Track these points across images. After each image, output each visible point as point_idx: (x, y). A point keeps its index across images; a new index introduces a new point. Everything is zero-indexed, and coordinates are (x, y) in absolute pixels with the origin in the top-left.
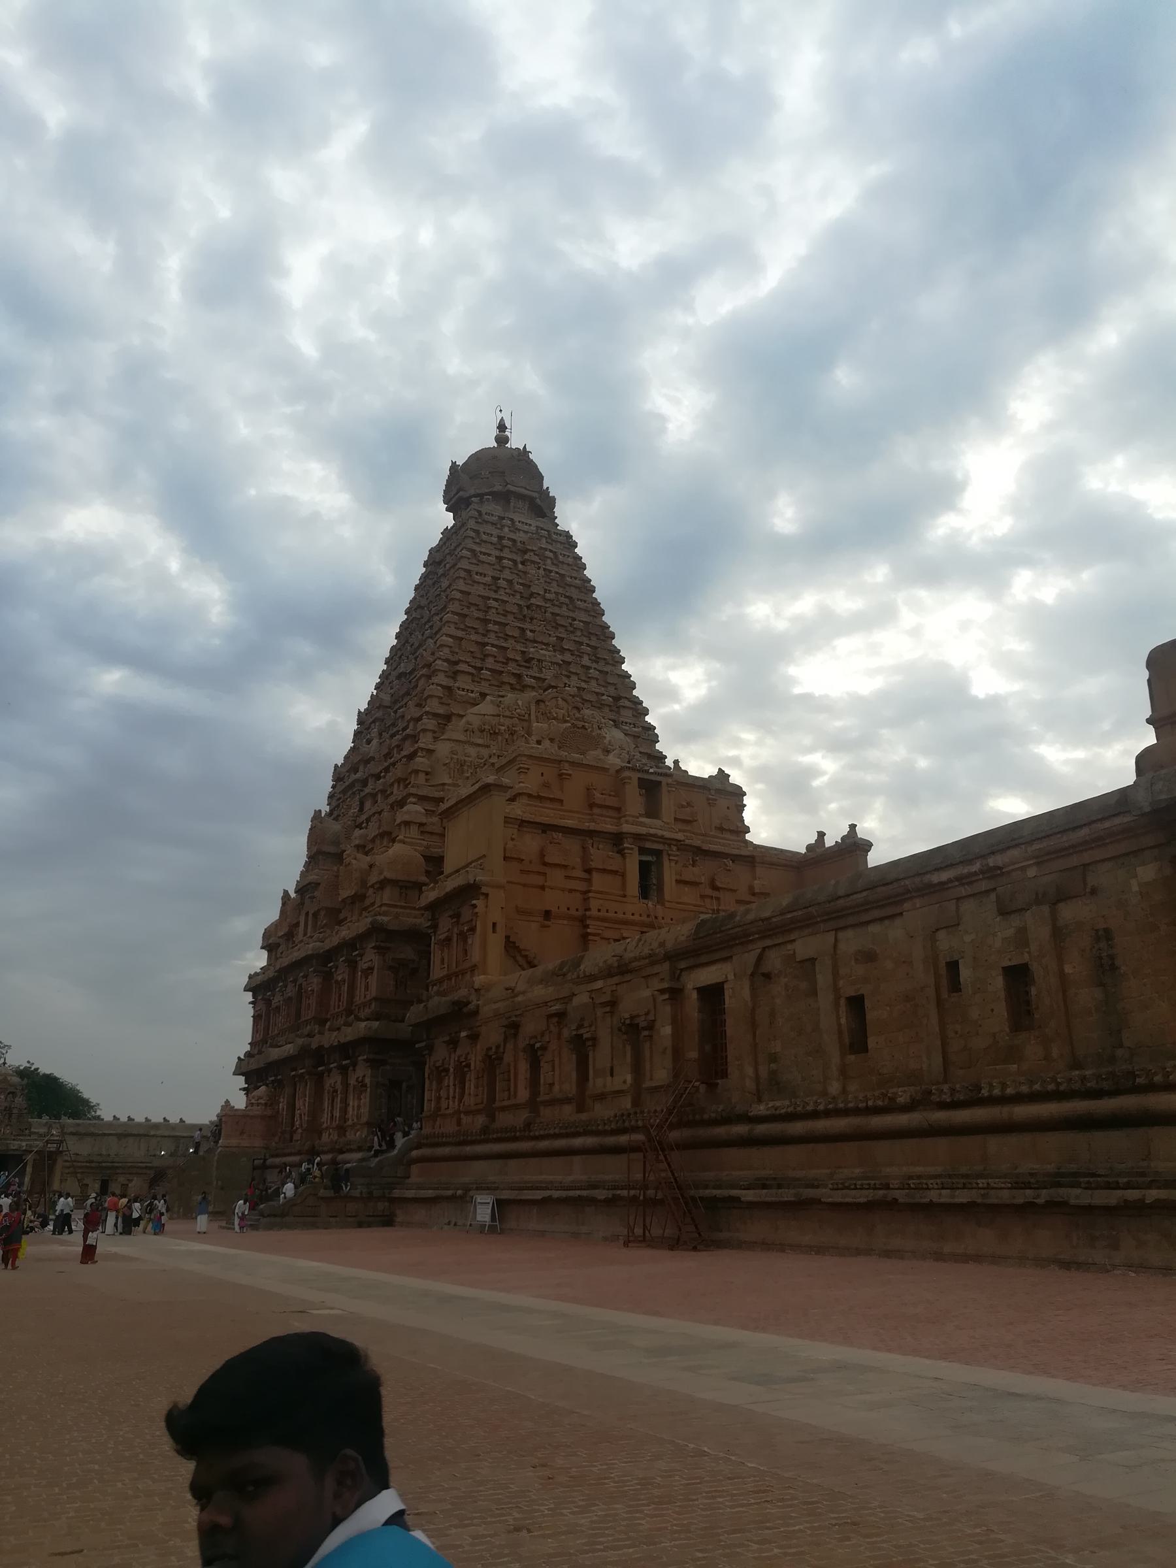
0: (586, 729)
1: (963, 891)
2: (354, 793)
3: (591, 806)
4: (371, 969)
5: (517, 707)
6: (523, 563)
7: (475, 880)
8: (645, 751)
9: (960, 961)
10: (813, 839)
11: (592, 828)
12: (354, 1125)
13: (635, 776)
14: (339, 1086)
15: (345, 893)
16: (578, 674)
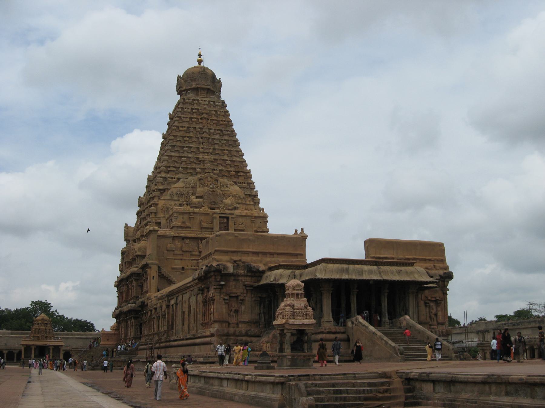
0: (214, 192)
1: (191, 289)
2: (139, 216)
3: (202, 228)
4: (133, 286)
5: (191, 183)
6: (201, 119)
7: (146, 263)
8: (247, 193)
9: (191, 306)
10: (294, 232)
11: (201, 237)
12: (131, 338)
13: (218, 216)
14: (130, 325)
15: (131, 257)
16: (221, 164)
